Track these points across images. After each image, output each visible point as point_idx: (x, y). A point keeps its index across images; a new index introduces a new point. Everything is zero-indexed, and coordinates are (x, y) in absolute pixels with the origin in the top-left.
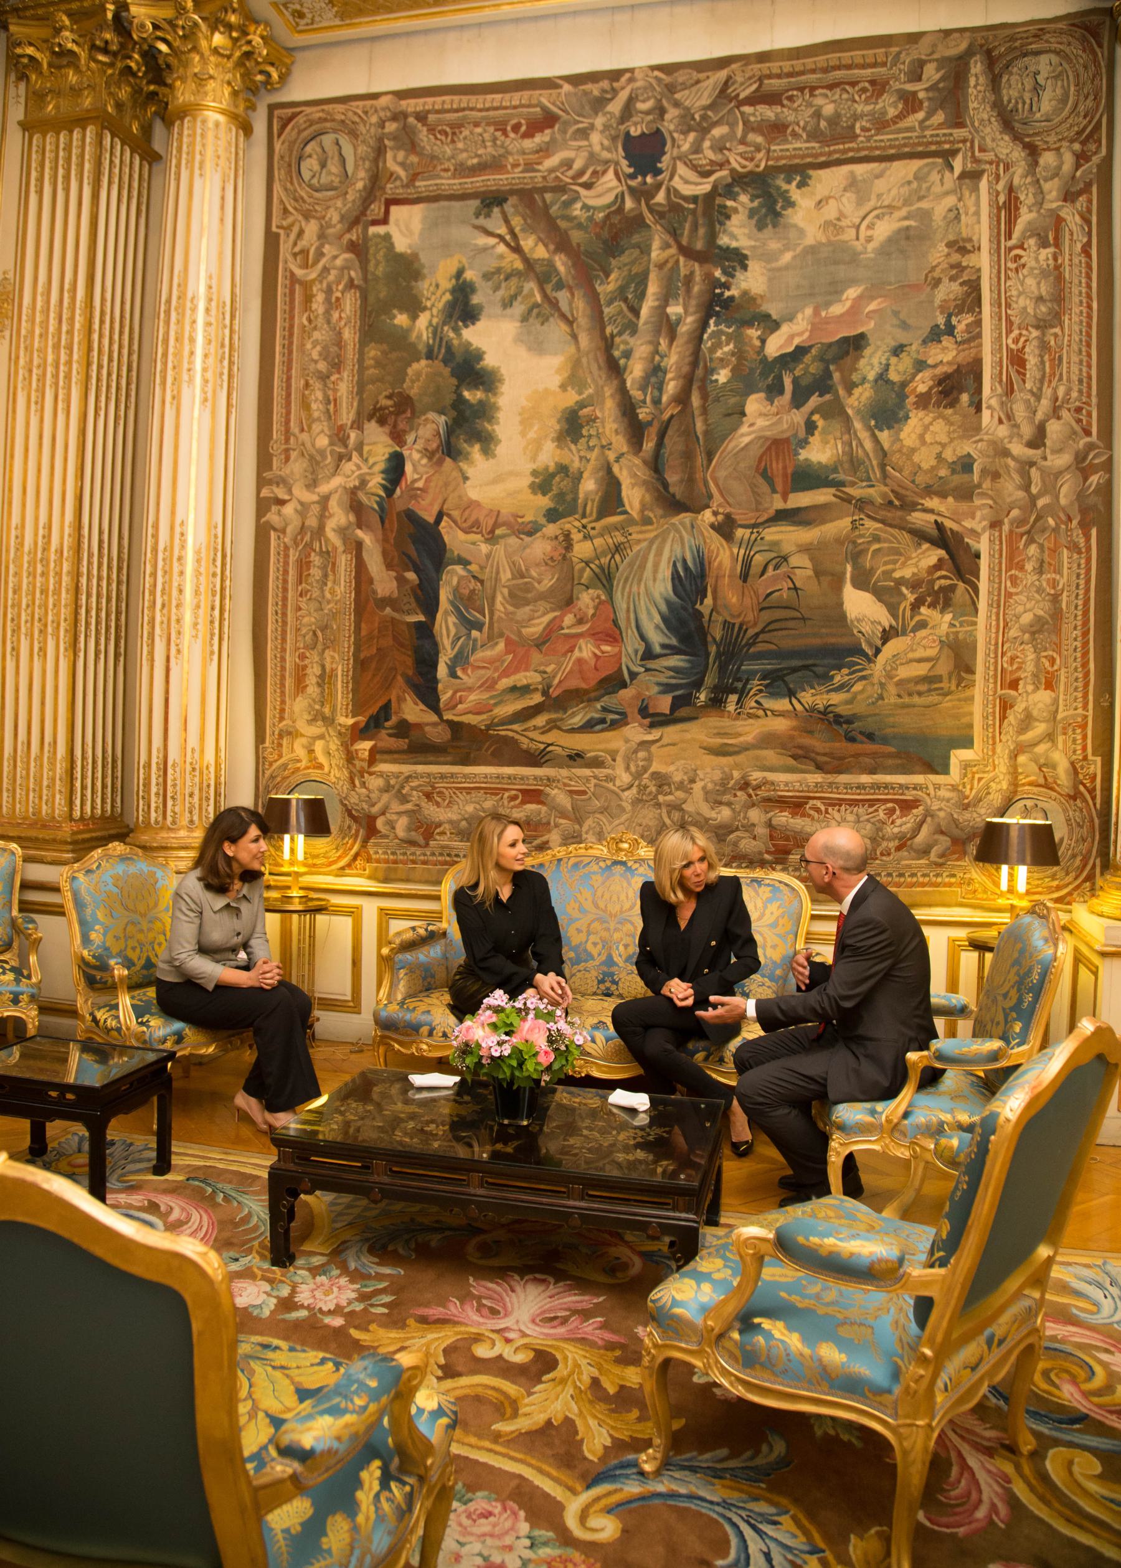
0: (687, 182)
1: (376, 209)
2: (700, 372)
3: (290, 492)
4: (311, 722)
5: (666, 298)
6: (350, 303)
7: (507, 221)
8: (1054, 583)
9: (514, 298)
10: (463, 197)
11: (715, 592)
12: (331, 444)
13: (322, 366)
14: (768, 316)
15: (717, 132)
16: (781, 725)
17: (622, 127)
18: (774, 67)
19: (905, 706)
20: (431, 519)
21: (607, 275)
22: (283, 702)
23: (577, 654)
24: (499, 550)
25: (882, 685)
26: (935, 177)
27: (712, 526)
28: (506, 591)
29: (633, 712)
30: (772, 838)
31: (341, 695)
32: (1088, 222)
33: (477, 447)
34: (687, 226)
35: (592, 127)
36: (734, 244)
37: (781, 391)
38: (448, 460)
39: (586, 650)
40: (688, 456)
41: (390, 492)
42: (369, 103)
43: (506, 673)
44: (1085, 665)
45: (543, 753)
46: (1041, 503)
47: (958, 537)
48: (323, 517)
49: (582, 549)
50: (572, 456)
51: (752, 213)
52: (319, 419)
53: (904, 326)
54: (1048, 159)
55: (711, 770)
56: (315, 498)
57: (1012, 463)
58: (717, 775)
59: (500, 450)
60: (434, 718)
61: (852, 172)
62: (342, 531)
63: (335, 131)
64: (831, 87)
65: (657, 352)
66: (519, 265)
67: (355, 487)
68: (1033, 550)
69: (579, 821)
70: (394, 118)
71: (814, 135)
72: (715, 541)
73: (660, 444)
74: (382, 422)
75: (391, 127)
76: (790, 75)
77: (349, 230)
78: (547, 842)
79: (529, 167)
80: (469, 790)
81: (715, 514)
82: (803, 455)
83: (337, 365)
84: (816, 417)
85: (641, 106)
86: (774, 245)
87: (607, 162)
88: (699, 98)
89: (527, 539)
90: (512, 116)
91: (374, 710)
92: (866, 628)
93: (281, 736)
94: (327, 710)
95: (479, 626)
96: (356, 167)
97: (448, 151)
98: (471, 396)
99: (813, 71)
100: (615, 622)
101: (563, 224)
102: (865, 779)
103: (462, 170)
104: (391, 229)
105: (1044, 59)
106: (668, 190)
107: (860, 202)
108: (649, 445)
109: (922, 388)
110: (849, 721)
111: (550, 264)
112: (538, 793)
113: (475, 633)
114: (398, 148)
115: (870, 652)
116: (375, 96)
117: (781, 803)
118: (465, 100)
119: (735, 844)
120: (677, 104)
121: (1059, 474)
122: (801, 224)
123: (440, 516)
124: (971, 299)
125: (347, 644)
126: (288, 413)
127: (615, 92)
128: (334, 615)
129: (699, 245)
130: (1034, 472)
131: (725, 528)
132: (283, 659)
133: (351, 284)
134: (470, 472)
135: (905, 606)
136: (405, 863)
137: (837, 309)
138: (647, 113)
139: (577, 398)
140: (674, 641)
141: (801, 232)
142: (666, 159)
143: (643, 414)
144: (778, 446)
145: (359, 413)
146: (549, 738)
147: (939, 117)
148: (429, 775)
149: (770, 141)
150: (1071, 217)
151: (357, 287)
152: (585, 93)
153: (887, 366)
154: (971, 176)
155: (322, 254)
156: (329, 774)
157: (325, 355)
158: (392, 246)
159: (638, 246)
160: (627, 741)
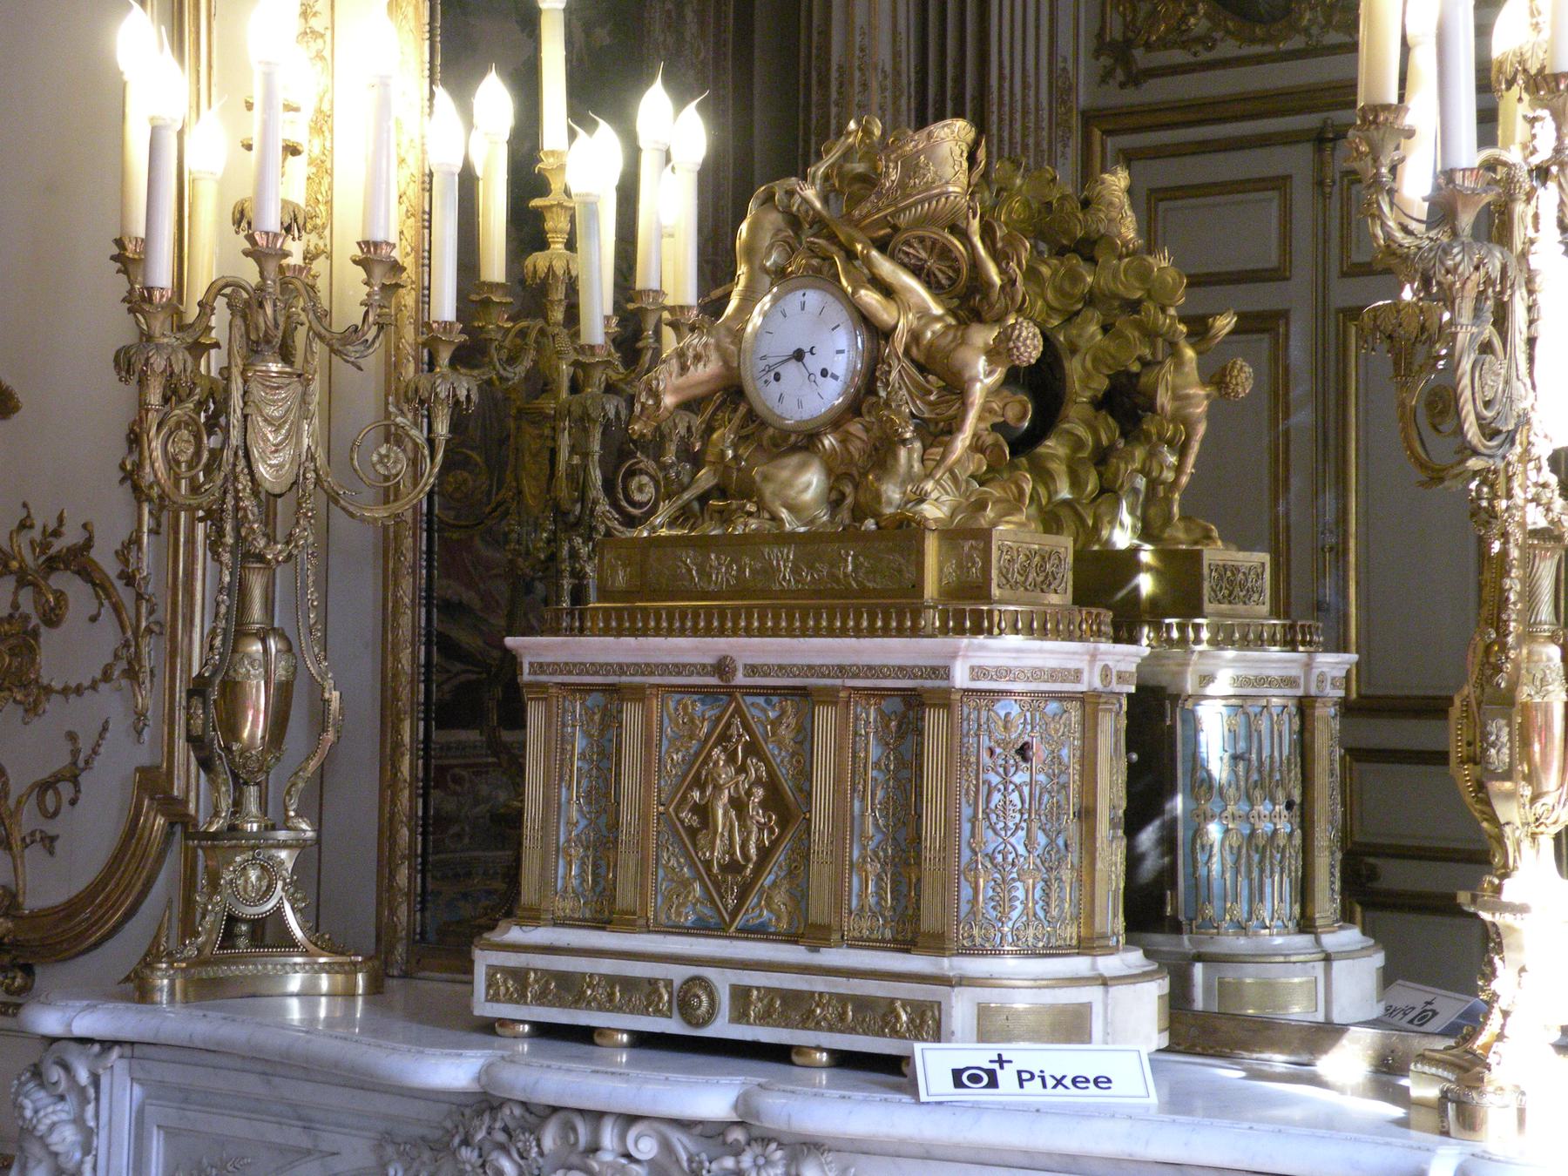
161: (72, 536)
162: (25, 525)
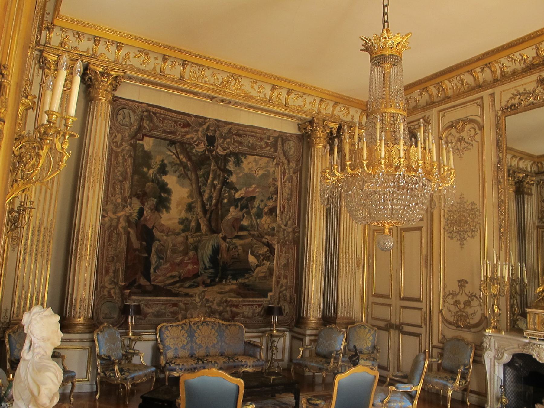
0: (220, 151)
2: (221, 199)
3: (107, 214)
4: (110, 284)
5: (214, 179)
6: (130, 162)
7: (176, 149)
10: (165, 139)
11: (221, 254)
12: (121, 202)
13: (120, 178)
14: (236, 188)
15: (228, 140)
16: (234, 287)
17: (206, 133)
20: (150, 227)
21: (201, 170)
22: (102, 278)
23: (188, 267)
24: (169, 238)
25: (256, 278)
26: (271, 163)
27: (221, 238)
28: (170, 250)
30: (231, 314)
32: (297, 179)
33: (164, 210)
34: (220, 162)
35: (199, 130)
36: (230, 169)
37: (238, 207)
38: (156, 212)
39: (190, 267)
43: (169, 272)
46: (286, 238)
48: (118, 222)
49: (191, 240)
50: (189, 216)
51: (234, 162)
52: (118, 194)
53: (263, 196)
54: (291, 164)
56: (116, 217)
57: (282, 230)
58: (220, 299)
59: (171, 211)
60: (149, 284)
61: (255, 158)
62: (123, 228)
63: (128, 109)
64: (252, 136)
65: (211, 192)
66: (178, 162)
67: (128, 216)
68: (284, 249)
70: (147, 111)
71: (248, 147)
73: (210, 216)
74: (138, 198)
75: (145, 113)
76: (244, 131)
77: (131, 140)
78: (178, 318)
79: (183, 136)
80: (157, 304)
81: (222, 235)
82: (242, 223)
83: (125, 179)
84: (245, 214)
85: (211, 128)
86: (238, 171)
87: (202, 140)
88: (225, 130)
89: (177, 236)
92: (253, 265)
93: (101, 288)
94: (116, 280)
95: (163, 259)
96: (134, 122)
99: (249, 132)
101: (190, 154)
102: (251, 299)
103: (164, 132)
104: (144, 143)
105: (292, 142)
106: (216, 152)
107: (257, 165)
108: (208, 216)
109: (266, 211)
111: (186, 163)
113: (161, 261)
114: (147, 120)
115: (253, 270)
116: (141, 103)
117: (234, 306)
118: (167, 113)
122: (244, 167)
123: (153, 227)
127: (205, 123)
129: (222, 167)
130: (285, 232)
131: (224, 238)
132: (102, 265)
134: (162, 216)
135: (261, 260)
137: (250, 189)
138: (212, 130)
139: (191, 200)
140: (211, 266)
141: (244, 169)
142: (216, 143)
143: (207, 207)
144: (238, 220)
147: (272, 150)
148: (147, 300)
151: (132, 157)
152: (198, 121)
153: (259, 205)
154: (277, 164)
155: (123, 145)
156: (115, 299)
157: (121, 175)
158: (144, 148)
160: (199, 290)
161: (474, 294)
162: (470, 292)
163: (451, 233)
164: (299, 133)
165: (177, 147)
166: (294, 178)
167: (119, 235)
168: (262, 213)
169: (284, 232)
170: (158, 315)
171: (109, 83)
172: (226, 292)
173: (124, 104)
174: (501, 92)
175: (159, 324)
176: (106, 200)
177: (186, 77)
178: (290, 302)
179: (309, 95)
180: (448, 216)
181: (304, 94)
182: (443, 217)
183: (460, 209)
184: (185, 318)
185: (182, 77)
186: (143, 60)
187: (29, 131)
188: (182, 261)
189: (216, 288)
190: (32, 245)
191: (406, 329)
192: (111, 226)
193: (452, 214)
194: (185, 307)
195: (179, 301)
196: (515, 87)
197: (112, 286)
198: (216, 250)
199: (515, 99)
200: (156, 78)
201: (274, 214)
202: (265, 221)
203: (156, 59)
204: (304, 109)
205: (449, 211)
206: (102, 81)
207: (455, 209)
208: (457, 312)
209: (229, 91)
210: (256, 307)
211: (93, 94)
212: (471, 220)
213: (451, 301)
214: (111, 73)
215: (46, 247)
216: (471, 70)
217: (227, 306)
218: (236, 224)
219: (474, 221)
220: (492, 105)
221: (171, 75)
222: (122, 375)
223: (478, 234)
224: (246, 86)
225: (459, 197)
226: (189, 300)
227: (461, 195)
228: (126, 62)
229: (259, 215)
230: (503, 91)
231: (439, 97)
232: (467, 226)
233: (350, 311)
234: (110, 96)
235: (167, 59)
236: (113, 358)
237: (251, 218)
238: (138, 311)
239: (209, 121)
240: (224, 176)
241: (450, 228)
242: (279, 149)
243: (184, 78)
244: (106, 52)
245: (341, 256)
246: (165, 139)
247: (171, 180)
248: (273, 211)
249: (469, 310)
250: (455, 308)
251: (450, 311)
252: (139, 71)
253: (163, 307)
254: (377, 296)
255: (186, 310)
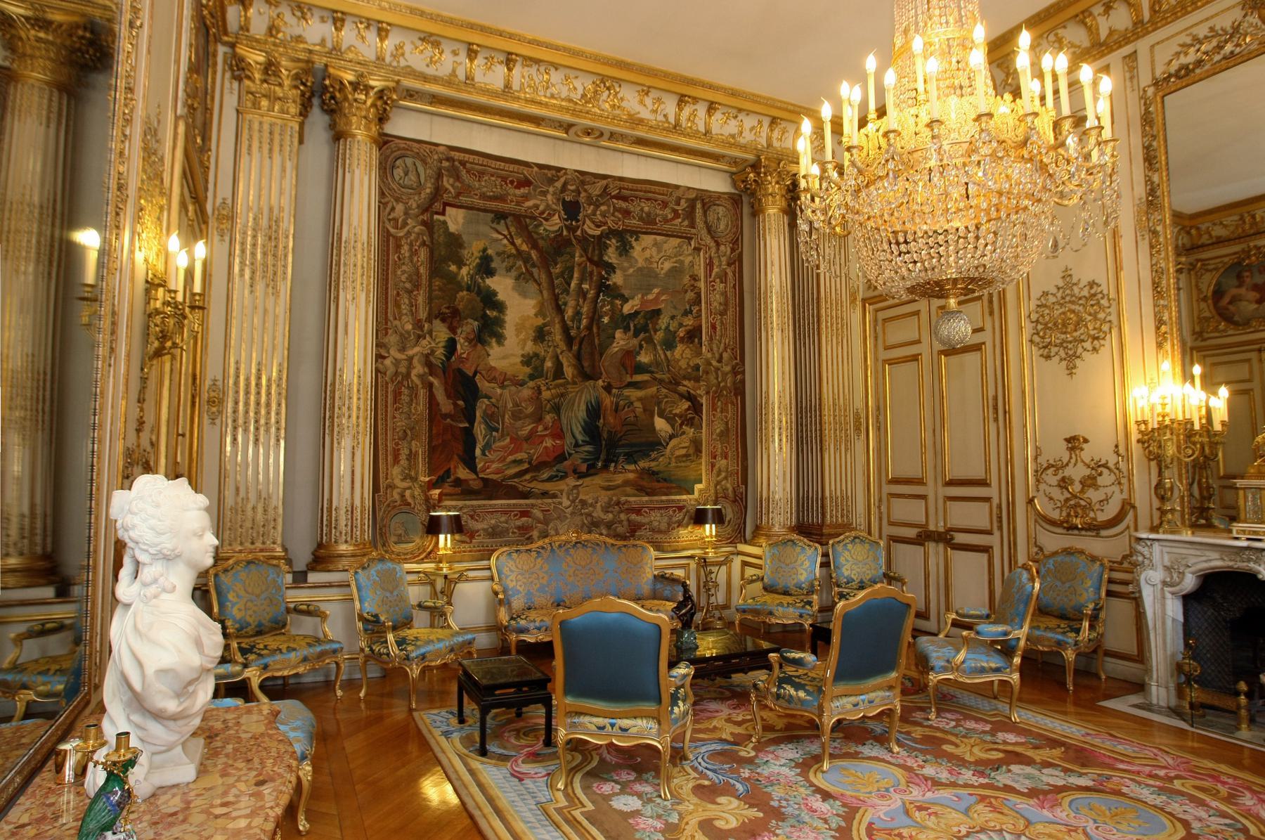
1: (438, 206)
2: (596, 317)
4: (402, 480)
5: (582, 280)
6: (423, 254)
7: (508, 229)
8: (726, 417)
9: (512, 267)
10: (485, 211)
13: (408, 285)
14: (623, 296)
15: (603, 208)
16: (631, 476)
18: (626, 185)
19: (677, 467)
20: (471, 375)
23: (544, 444)
24: (506, 392)
26: (685, 247)
29: (570, 472)
31: (421, 465)
33: (494, 340)
35: (548, 191)
39: (549, 443)
40: (592, 354)
41: (448, 358)
42: (433, 147)
43: (511, 454)
44: (737, 449)
45: (530, 492)
47: (695, 397)
48: (410, 367)
49: (546, 394)
51: (617, 248)
53: (675, 308)
54: (722, 248)
55: (604, 497)
56: (404, 357)
58: (606, 499)
59: (506, 343)
60: (475, 477)
61: (655, 239)
62: (420, 376)
63: (413, 157)
64: (648, 199)
66: (514, 251)
68: (719, 403)
69: (547, 525)
70: (448, 159)
71: (641, 219)
72: (604, 394)
73: (580, 348)
74: (443, 320)
75: (445, 164)
77: (422, 213)
79: (518, 204)
82: (638, 358)
83: (417, 286)
85: (570, 187)
86: (626, 264)
88: (596, 190)
90: (510, 176)
91: (441, 473)
92: (663, 434)
94: (413, 474)
95: (497, 430)
96: (426, 180)
97: (477, 184)
98: (491, 313)
100: (562, 430)
101: (535, 236)
102: (664, 498)
103: (483, 197)
104: (446, 218)
105: (721, 208)
107: (659, 251)
108: (575, 348)
109: (682, 335)
110: (657, 473)
111: (529, 254)
112: (528, 512)
116: (437, 145)
118: (486, 161)
119: (615, 530)
120: (586, 191)
121: (727, 374)
123: (475, 373)
124: (697, 301)
125: (424, 438)
126: (387, 308)
127: (559, 178)
128: (417, 422)
129: (596, 258)
130: (719, 372)
131: (608, 388)
132: (386, 446)
133: (424, 244)
134: (491, 352)
136: (459, 552)
137: (650, 297)
138: (573, 191)
140: (588, 439)
141: (636, 261)
143: (573, 333)
144: (629, 354)
145: (429, 314)
146: (532, 485)
147: (686, 223)
149: (624, 218)
150: (729, 271)
152: (544, 174)
154: (697, 249)
155: (407, 224)
157: (410, 279)
158: (447, 228)
159: (569, 253)
161: (1103, 462)
163: (1045, 347)
164: (733, 191)
165: (509, 223)
166: (730, 274)
167: (413, 389)
168: (674, 341)
169: (717, 374)
170: (494, 533)
171: (369, 102)
172: (617, 487)
173: (404, 149)
174: (1152, 46)
175: (494, 551)
176: (383, 326)
177: (516, 86)
178: (735, 501)
179: (749, 112)
180: (1037, 316)
181: (740, 110)
182: (1027, 320)
183: (1063, 298)
184: (546, 537)
185: (508, 86)
186: (431, 58)
187: (224, 199)
188: (533, 432)
189: (598, 480)
190: (247, 412)
191: (960, 538)
192: (396, 373)
193: (1047, 311)
194: (544, 515)
195: (533, 506)
196: (1186, 29)
197: (405, 484)
198: (594, 412)
199: (1186, 54)
200: (459, 90)
201: (696, 340)
202: (681, 353)
203: (455, 53)
204: (742, 141)
205: (1038, 306)
206: (356, 100)
207: (1052, 299)
208: (1067, 500)
209: (596, 110)
210: (674, 511)
211: (341, 126)
212: (1090, 318)
213: (1051, 478)
214: (372, 83)
215: (273, 414)
216: (1083, 12)
217: (622, 512)
218: (628, 361)
219: (1096, 319)
220: (1131, 78)
221: (486, 84)
222: (402, 650)
223: (1107, 343)
224: (630, 100)
225: (1062, 275)
226: (550, 504)
227: (1066, 270)
228: (398, 62)
229: (669, 344)
230: (1158, 43)
231: (1010, 85)
232: (1082, 331)
233: (848, 511)
234: (374, 129)
235: (476, 52)
236: (382, 618)
237: (655, 349)
238: (457, 526)
239: (565, 174)
240: (600, 273)
241: (1043, 338)
242: (698, 221)
243: (511, 88)
244: (358, 43)
245: (826, 412)
246: (485, 211)
247: (501, 285)
248: (693, 335)
249: (1093, 495)
250: (1062, 493)
251: (1051, 499)
252: (425, 78)
253: (503, 519)
254: (896, 481)
255: (546, 522)
